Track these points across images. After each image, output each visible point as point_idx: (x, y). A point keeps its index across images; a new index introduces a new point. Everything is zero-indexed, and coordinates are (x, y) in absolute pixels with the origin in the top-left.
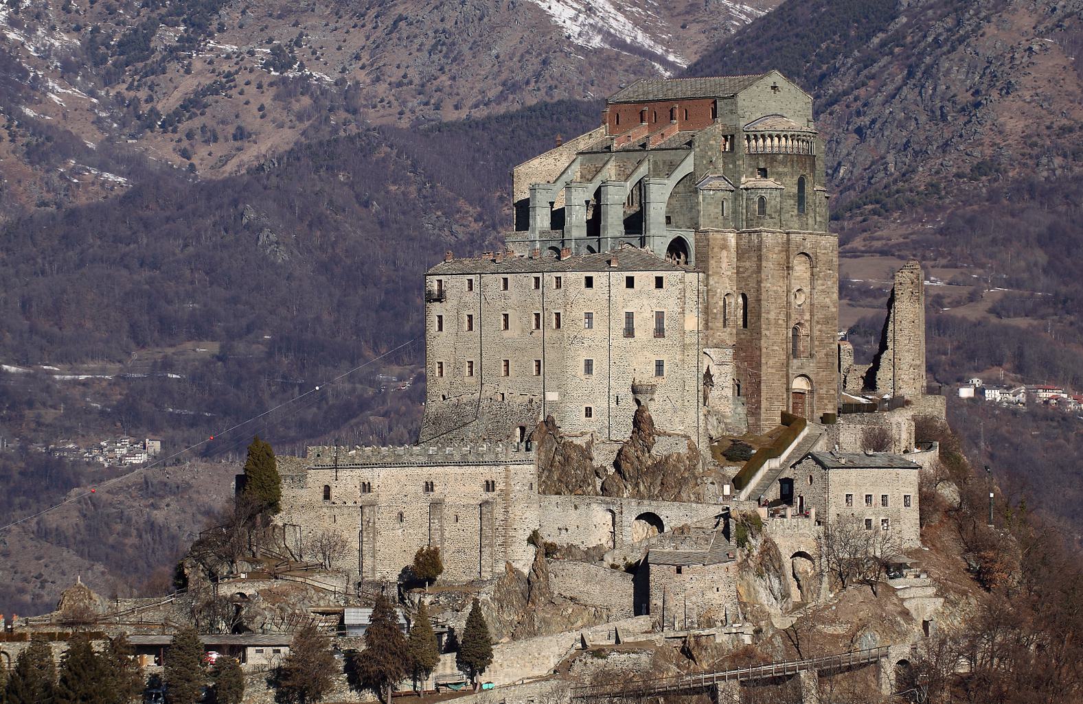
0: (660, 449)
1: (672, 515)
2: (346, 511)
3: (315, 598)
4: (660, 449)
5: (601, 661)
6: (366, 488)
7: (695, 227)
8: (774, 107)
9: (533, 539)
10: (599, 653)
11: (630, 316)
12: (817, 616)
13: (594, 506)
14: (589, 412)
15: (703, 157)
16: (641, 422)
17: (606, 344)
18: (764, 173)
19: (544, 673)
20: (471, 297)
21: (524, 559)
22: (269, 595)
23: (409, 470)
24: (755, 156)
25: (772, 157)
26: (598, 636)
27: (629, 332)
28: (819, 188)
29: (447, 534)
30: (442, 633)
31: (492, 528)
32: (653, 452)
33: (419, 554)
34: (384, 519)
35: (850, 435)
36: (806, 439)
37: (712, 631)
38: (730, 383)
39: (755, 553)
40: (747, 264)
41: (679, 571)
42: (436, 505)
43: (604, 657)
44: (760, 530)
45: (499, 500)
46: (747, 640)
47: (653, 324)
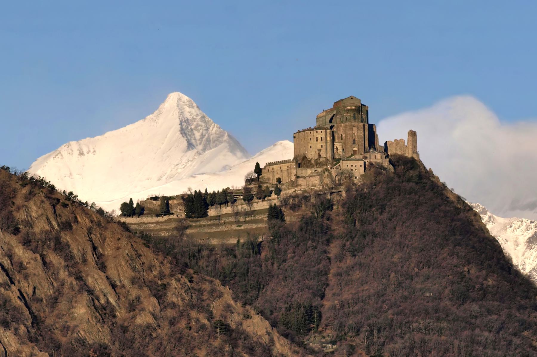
4: (321, 159)
16: (320, 156)
21: (293, 178)
27: (317, 140)
31: (289, 174)
34: (275, 174)
42: (282, 171)
46: (321, 188)
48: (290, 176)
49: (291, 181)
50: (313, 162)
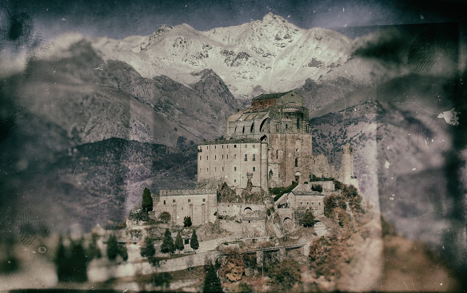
0: (254, 190)
1: (254, 207)
2: (169, 207)
3: (159, 230)
4: (254, 190)
5: (226, 246)
6: (174, 201)
7: (269, 133)
8: (292, 100)
9: (215, 214)
10: (226, 244)
11: (246, 155)
12: (290, 235)
13: (234, 205)
14: (235, 181)
15: (271, 114)
16: (250, 183)
17: (240, 162)
18: (288, 118)
19: (213, 249)
20: (208, 151)
21: (213, 219)
22: (146, 229)
23: (184, 196)
24: (285, 113)
25: (289, 113)
26: (228, 239)
27: (246, 160)
28: (304, 121)
29: (194, 213)
30: (189, 239)
32: (252, 191)
33: (185, 218)
34: (179, 209)
35: (308, 187)
36: (297, 188)
37: (258, 238)
38: (278, 174)
39: (273, 217)
40: (283, 142)
41: (249, 222)
42: (191, 205)
43: (227, 245)
44: (274, 211)
45: (206, 204)
47: (252, 157)
48: (208, 215)
49: (210, 223)
50: (238, 193)
